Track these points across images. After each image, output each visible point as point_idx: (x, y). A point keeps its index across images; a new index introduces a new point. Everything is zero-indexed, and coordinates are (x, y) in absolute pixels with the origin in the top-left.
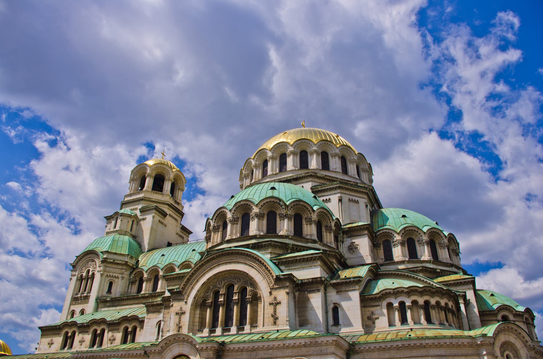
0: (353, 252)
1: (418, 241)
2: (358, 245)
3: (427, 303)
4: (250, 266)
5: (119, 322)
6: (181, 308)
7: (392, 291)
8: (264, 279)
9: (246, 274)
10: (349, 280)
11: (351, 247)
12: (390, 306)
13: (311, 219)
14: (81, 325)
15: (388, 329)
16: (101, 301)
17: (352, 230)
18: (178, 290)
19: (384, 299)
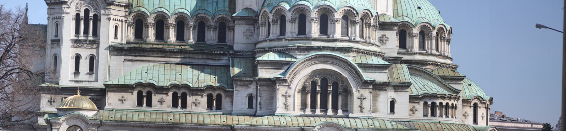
0: (383, 43)
1: (428, 35)
2: (388, 38)
3: (447, 104)
4: (343, 69)
5: (203, 89)
6: (286, 92)
7: (429, 95)
8: (354, 80)
9: (339, 74)
10: (405, 85)
11: (381, 39)
12: (426, 103)
13: (370, 24)
14: (159, 87)
15: (422, 118)
16: (116, 48)
17: (385, 24)
18: (285, 79)
19: (423, 99)
